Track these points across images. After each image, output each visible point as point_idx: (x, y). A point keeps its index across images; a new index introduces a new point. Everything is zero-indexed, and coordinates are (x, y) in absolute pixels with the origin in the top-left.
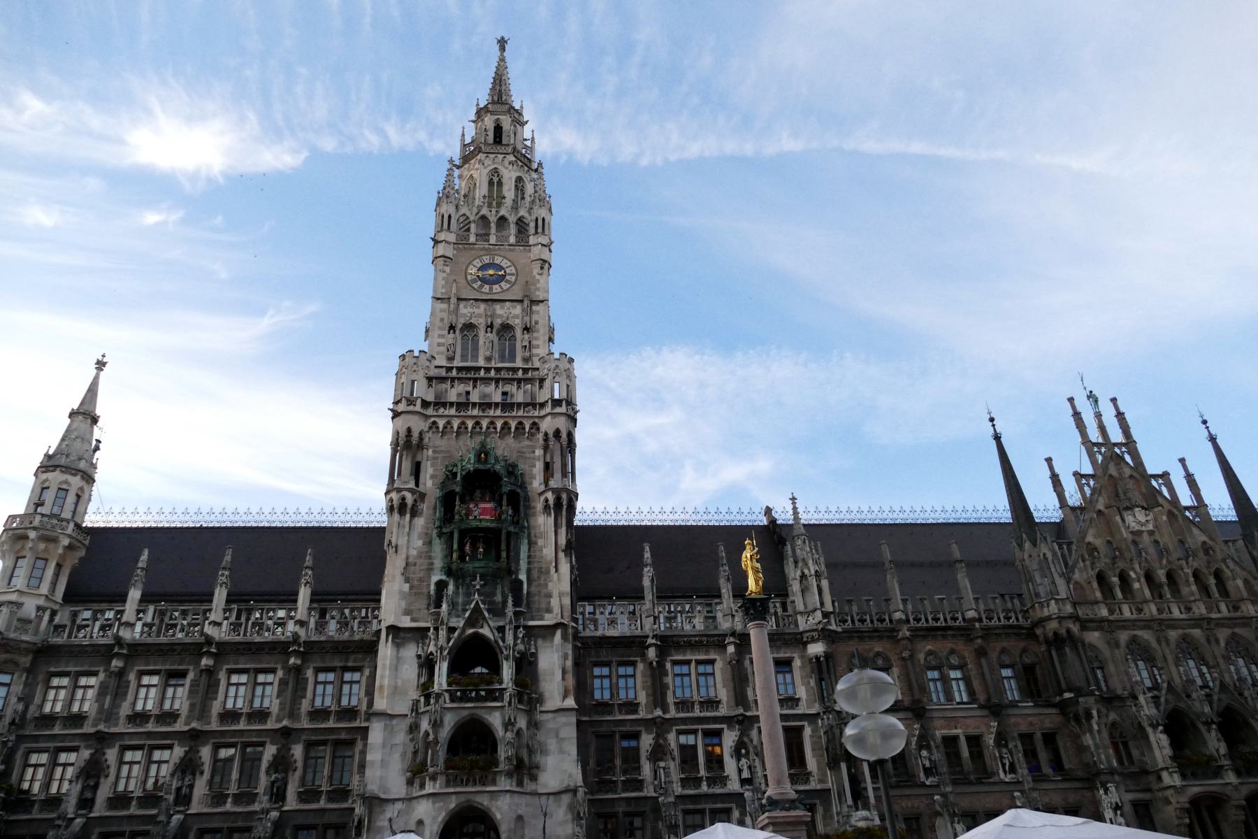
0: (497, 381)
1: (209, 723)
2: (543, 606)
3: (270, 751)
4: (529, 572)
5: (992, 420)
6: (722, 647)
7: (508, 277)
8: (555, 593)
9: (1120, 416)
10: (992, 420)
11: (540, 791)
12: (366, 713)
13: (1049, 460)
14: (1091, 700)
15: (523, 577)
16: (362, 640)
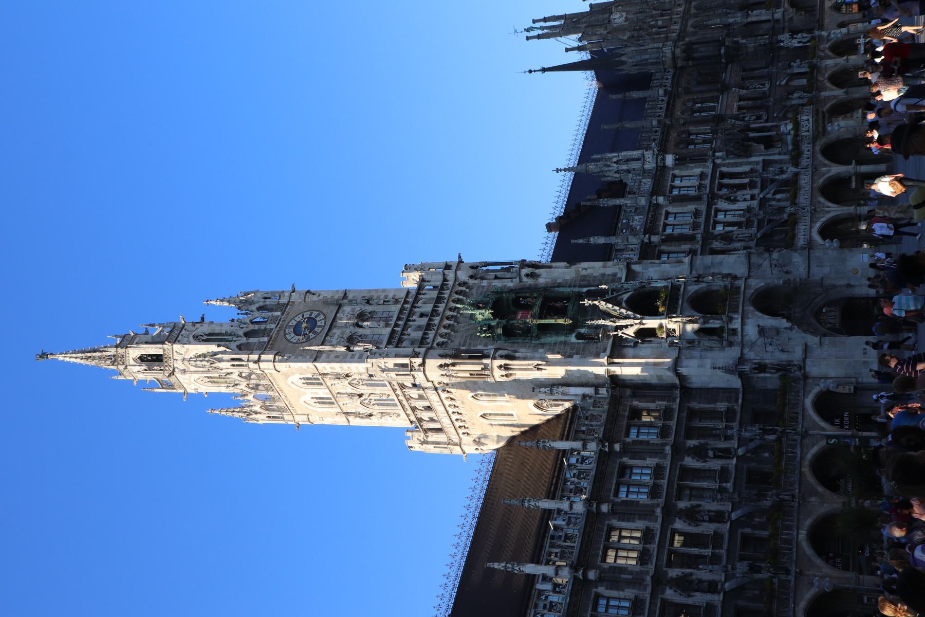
0: (408, 320)
1: (658, 505)
2: (610, 278)
3: (689, 462)
4: (581, 286)
5: (530, 71)
6: (658, 206)
7: (313, 316)
8: (602, 271)
9: (545, 20)
10: (530, 71)
11: (746, 275)
12: (669, 401)
13: (567, 50)
14: (727, 39)
15: (585, 290)
16: (609, 404)
